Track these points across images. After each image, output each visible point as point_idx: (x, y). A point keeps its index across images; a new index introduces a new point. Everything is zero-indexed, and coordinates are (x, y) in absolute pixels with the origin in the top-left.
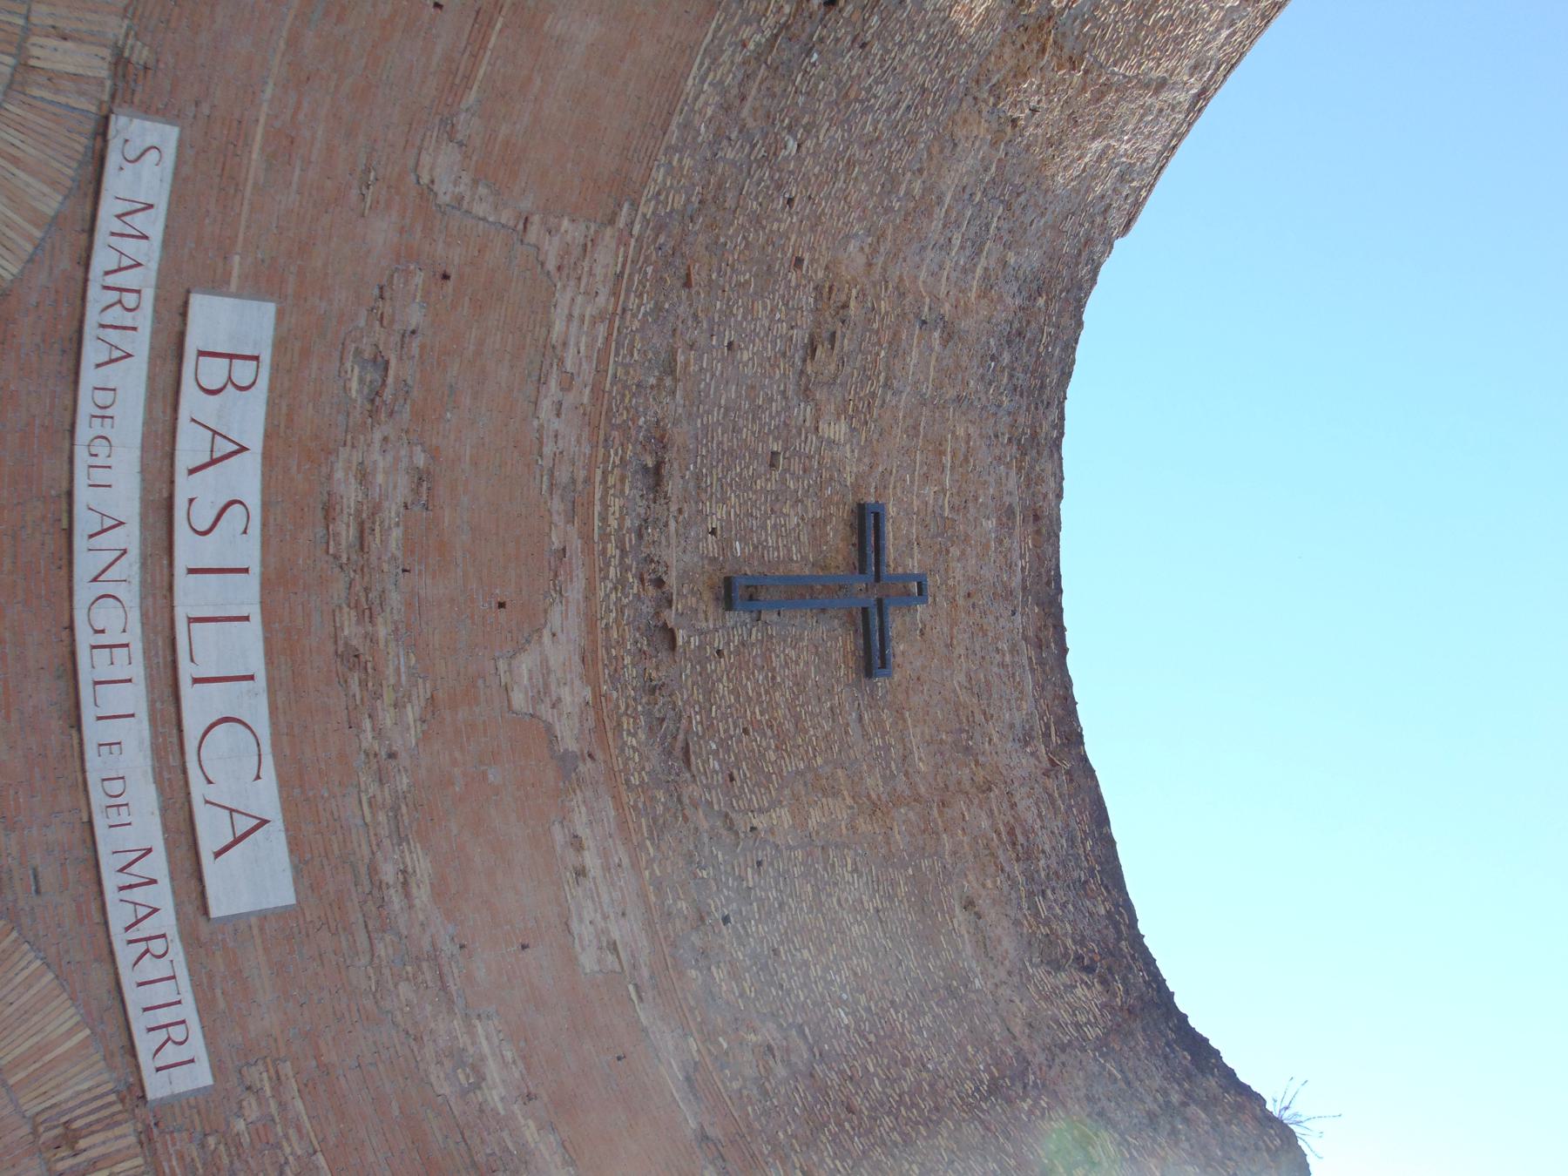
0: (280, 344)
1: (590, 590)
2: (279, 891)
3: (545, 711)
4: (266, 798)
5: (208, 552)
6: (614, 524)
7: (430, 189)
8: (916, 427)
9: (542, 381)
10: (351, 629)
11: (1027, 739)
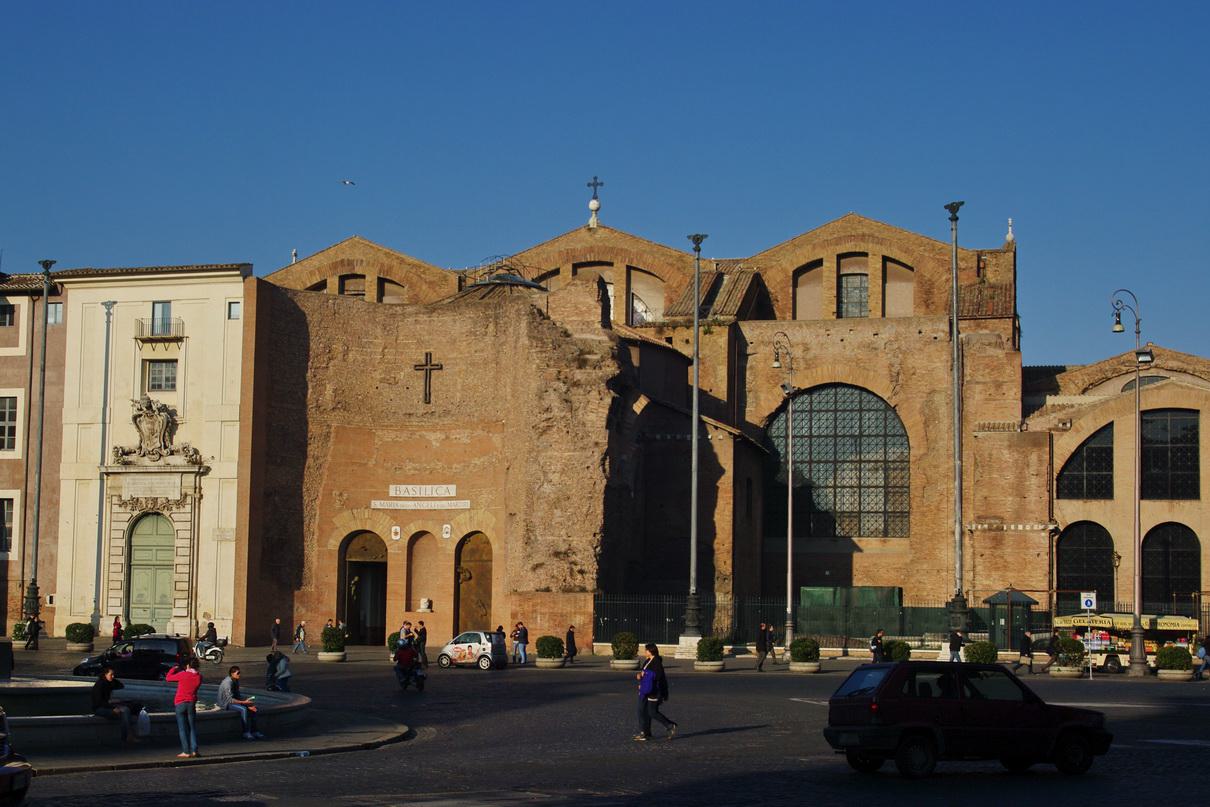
0: (394, 484)
1: (426, 431)
2: (454, 487)
4: (445, 486)
7: (374, 465)
10: (428, 472)
11: (455, 321)
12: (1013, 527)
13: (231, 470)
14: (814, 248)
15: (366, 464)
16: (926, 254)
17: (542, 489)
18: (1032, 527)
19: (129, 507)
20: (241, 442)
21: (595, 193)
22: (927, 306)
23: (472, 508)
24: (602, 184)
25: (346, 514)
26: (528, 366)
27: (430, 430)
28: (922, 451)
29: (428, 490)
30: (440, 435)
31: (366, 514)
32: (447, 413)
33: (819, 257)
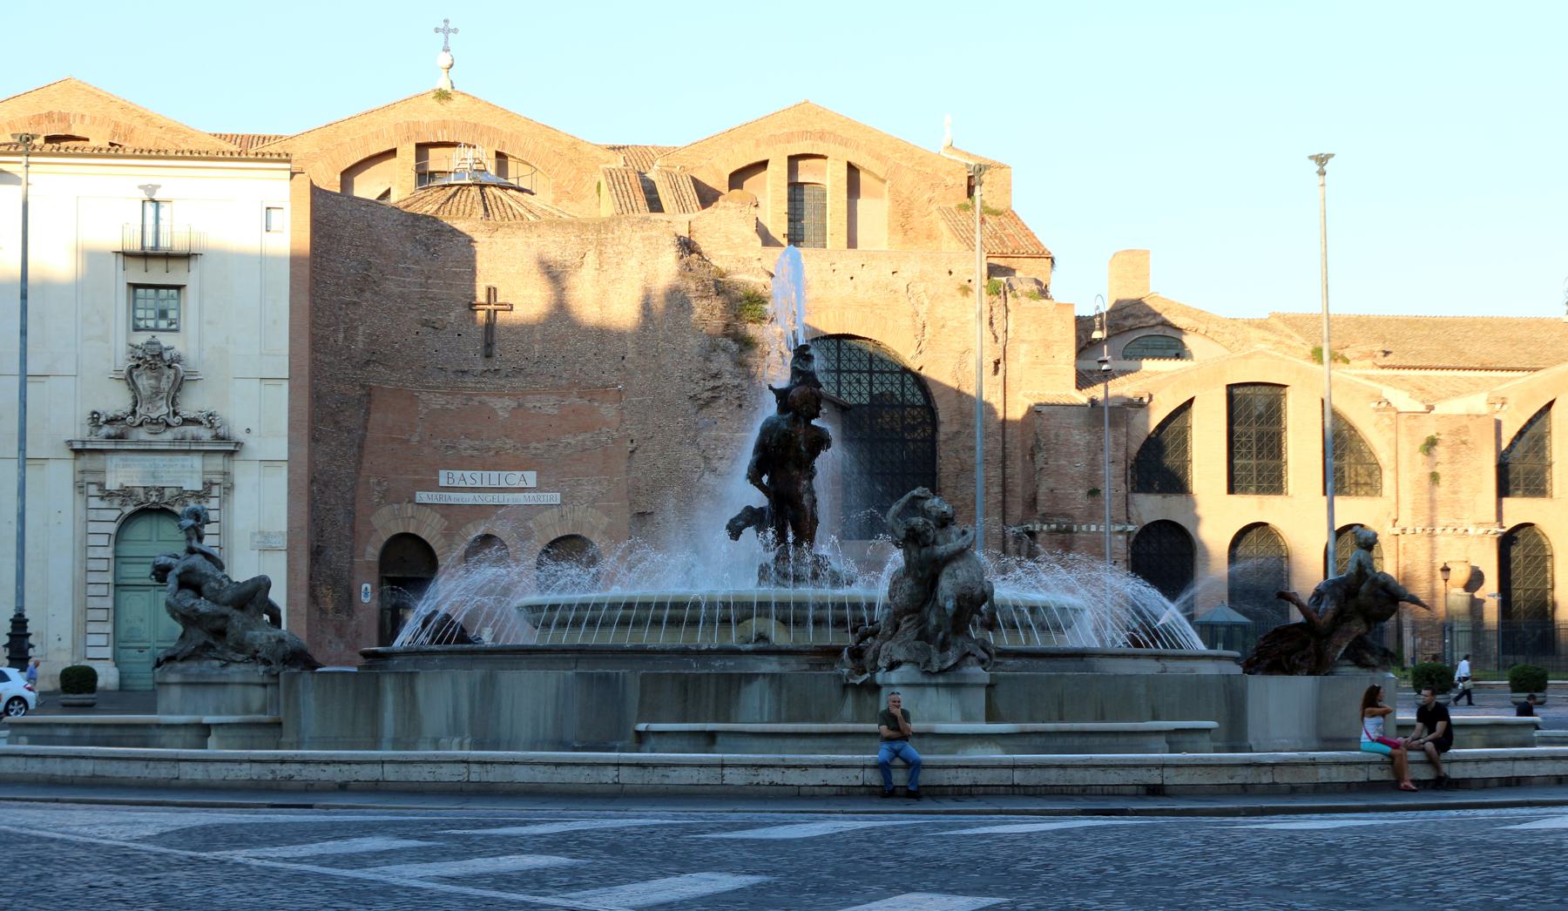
0: (446, 468)
3: (510, 409)
4: (518, 474)
5: (479, 481)
6: (473, 385)
8: (450, 284)
9: (447, 409)
10: (492, 453)
12: (1084, 528)
13: (279, 447)
14: (758, 144)
15: (408, 440)
16: (904, 163)
17: (702, 480)
19: (117, 502)
20: (291, 409)
21: (446, 42)
22: (905, 233)
23: (563, 503)
24: (455, 31)
25: (385, 511)
26: (682, 316)
27: (495, 394)
28: (955, 428)
29: (493, 478)
30: (509, 403)
31: (410, 511)
32: (518, 371)
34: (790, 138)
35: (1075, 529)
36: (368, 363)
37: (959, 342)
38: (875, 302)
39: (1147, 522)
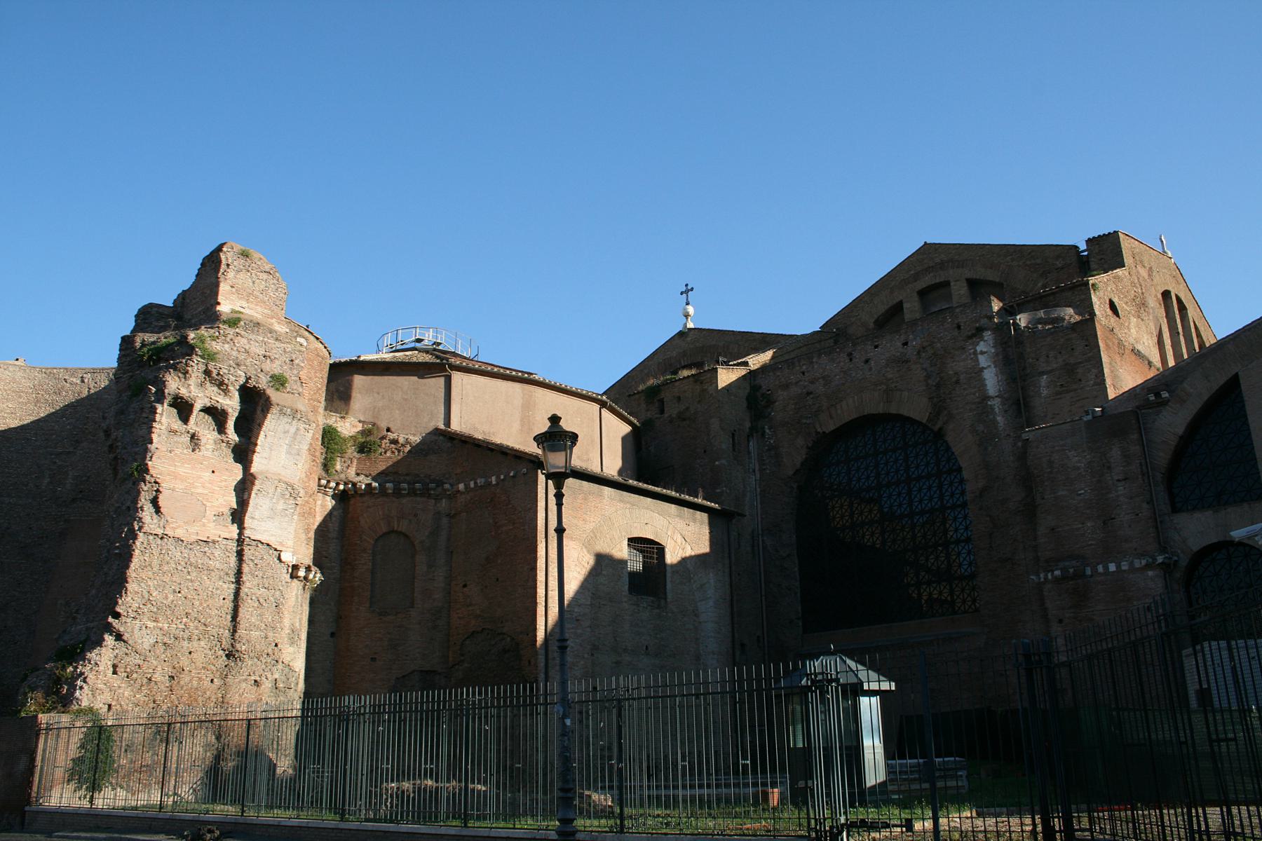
12: (1100, 569)
18: (1131, 564)
21: (687, 299)
33: (898, 300)
34: (916, 277)
35: (1088, 571)
36: (74, 500)
37: (974, 394)
38: (890, 376)
39: (1196, 548)
